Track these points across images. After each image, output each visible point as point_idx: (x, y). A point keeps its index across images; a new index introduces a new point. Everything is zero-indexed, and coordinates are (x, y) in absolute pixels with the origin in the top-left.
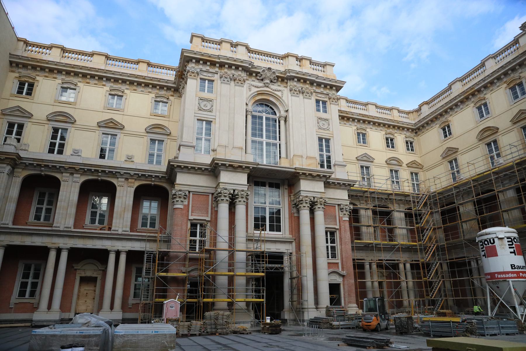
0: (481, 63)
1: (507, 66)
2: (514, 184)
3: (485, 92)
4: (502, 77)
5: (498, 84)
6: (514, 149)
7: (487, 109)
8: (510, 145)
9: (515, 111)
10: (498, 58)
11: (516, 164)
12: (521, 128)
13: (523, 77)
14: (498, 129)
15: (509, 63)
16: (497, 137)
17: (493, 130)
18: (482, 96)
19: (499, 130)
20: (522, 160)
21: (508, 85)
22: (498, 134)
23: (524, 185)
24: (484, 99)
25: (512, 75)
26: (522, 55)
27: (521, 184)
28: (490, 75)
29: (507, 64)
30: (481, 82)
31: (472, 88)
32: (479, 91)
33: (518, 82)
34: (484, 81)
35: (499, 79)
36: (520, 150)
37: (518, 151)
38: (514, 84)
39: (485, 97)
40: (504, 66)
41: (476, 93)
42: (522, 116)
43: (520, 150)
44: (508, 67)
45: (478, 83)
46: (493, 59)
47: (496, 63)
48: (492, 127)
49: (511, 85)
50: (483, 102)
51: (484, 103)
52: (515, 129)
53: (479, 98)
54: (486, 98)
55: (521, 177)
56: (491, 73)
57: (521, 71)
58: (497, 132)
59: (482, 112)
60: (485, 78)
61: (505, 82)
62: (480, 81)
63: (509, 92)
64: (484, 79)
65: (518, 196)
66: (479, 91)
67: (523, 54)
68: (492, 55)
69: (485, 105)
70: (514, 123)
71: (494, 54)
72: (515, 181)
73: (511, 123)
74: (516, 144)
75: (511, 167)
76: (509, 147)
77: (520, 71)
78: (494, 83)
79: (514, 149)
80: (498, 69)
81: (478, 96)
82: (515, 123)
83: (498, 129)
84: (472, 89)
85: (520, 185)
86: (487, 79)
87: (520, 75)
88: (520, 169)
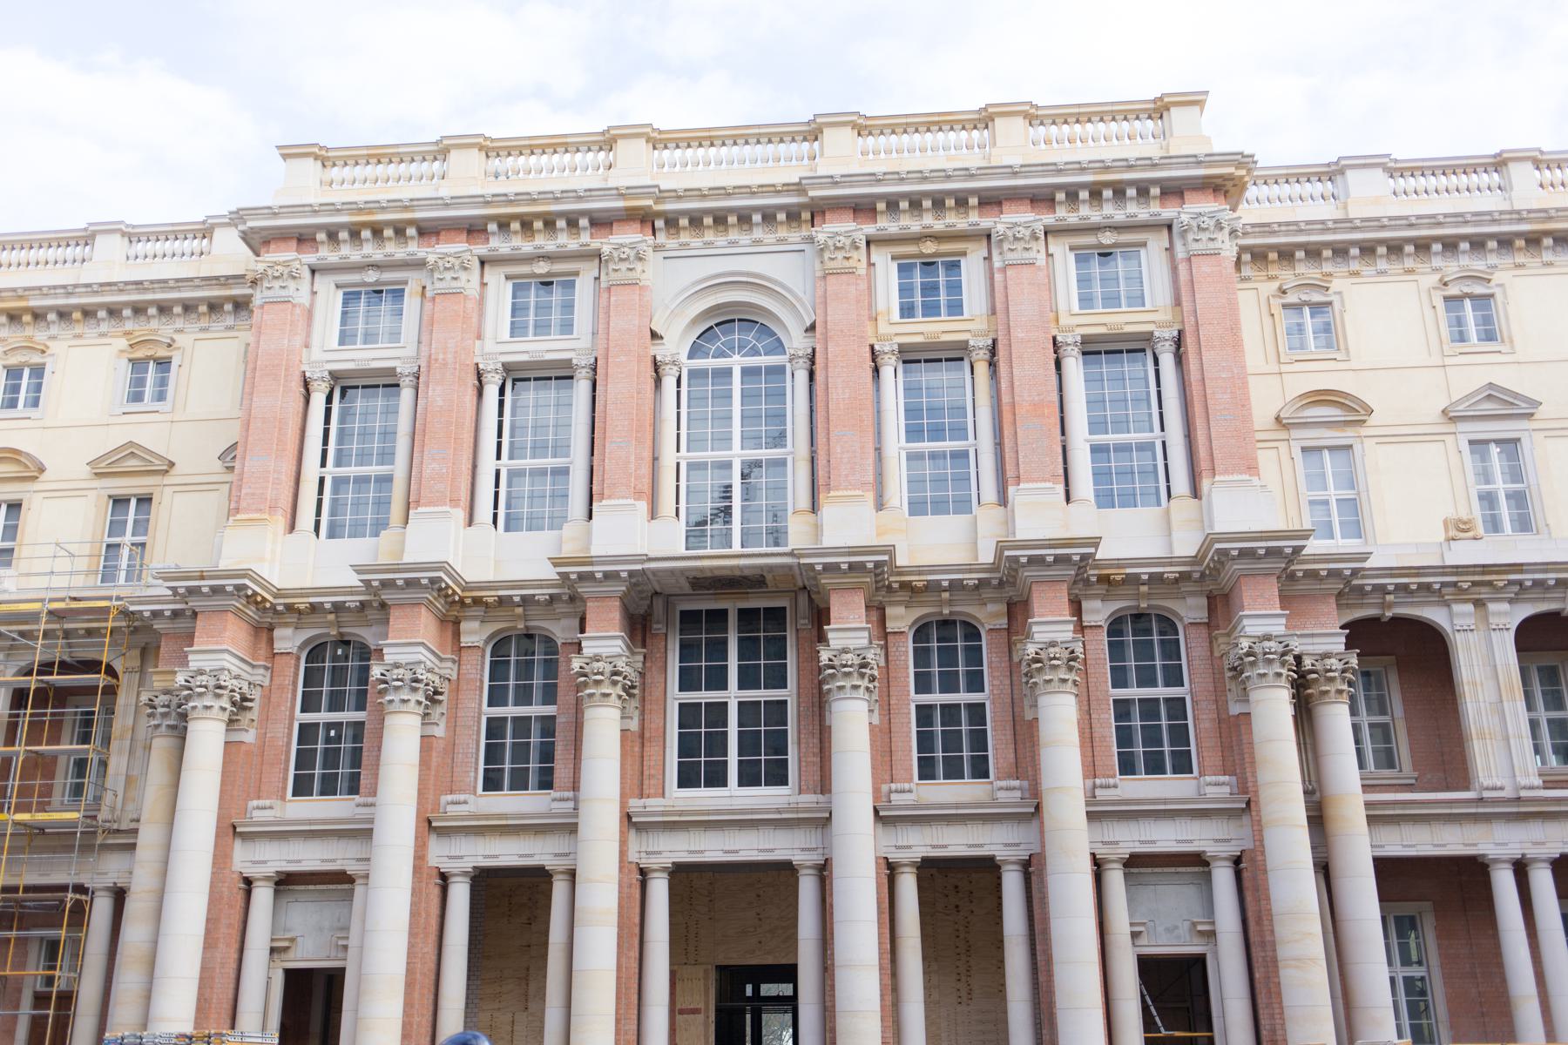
0: (85, 230)
1: (153, 290)
2: (14, 670)
3: (54, 330)
4: (127, 312)
5: (104, 327)
6: (63, 564)
7: (38, 388)
8: (57, 544)
9: (115, 438)
10: (140, 248)
11: (50, 613)
12: (110, 497)
13: (179, 348)
14: (42, 470)
15: (162, 285)
16: (28, 495)
17: (26, 466)
18: (39, 335)
19: (44, 477)
20: (74, 605)
21: (130, 345)
22: (36, 486)
23: (44, 685)
24: (43, 352)
25: (154, 324)
26: (204, 283)
27: (37, 681)
28: (95, 288)
29: (156, 286)
30: (58, 291)
31: (20, 293)
32: (38, 316)
33: (162, 352)
34: (69, 294)
35: (114, 312)
36: (78, 573)
37: (71, 573)
38: (150, 353)
39: (48, 347)
40: (146, 285)
41: (27, 318)
42: (126, 464)
43: (78, 573)
44: (154, 293)
45: (45, 291)
46: (126, 239)
47: (128, 258)
48: (28, 455)
49: (139, 354)
50: (36, 359)
51: (37, 364)
52: (92, 494)
53: (30, 339)
54: (48, 352)
55: (47, 658)
56: (102, 285)
57: (181, 326)
58: (37, 478)
59: (16, 389)
60: (76, 286)
61: (127, 333)
62: (55, 287)
63: (125, 369)
64: (70, 289)
65: (10, 716)
66: (38, 316)
67: (208, 282)
68: (127, 226)
69: (38, 371)
70: (96, 474)
71: (134, 227)
72: (23, 664)
73: (88, 468)
74: (73, 548)
75: (33, 617)
76: (50, 550)
77: (179, 323)
78: (96, 317)
79: (63, 564)
80: (126, 283)
81: (29, 331)
82: (99, 475)
83: (42, 470)
84: (21, 298)
85: (33, 682)
86: (80, 295)
87: (175, 337)
88: (54, 630)
